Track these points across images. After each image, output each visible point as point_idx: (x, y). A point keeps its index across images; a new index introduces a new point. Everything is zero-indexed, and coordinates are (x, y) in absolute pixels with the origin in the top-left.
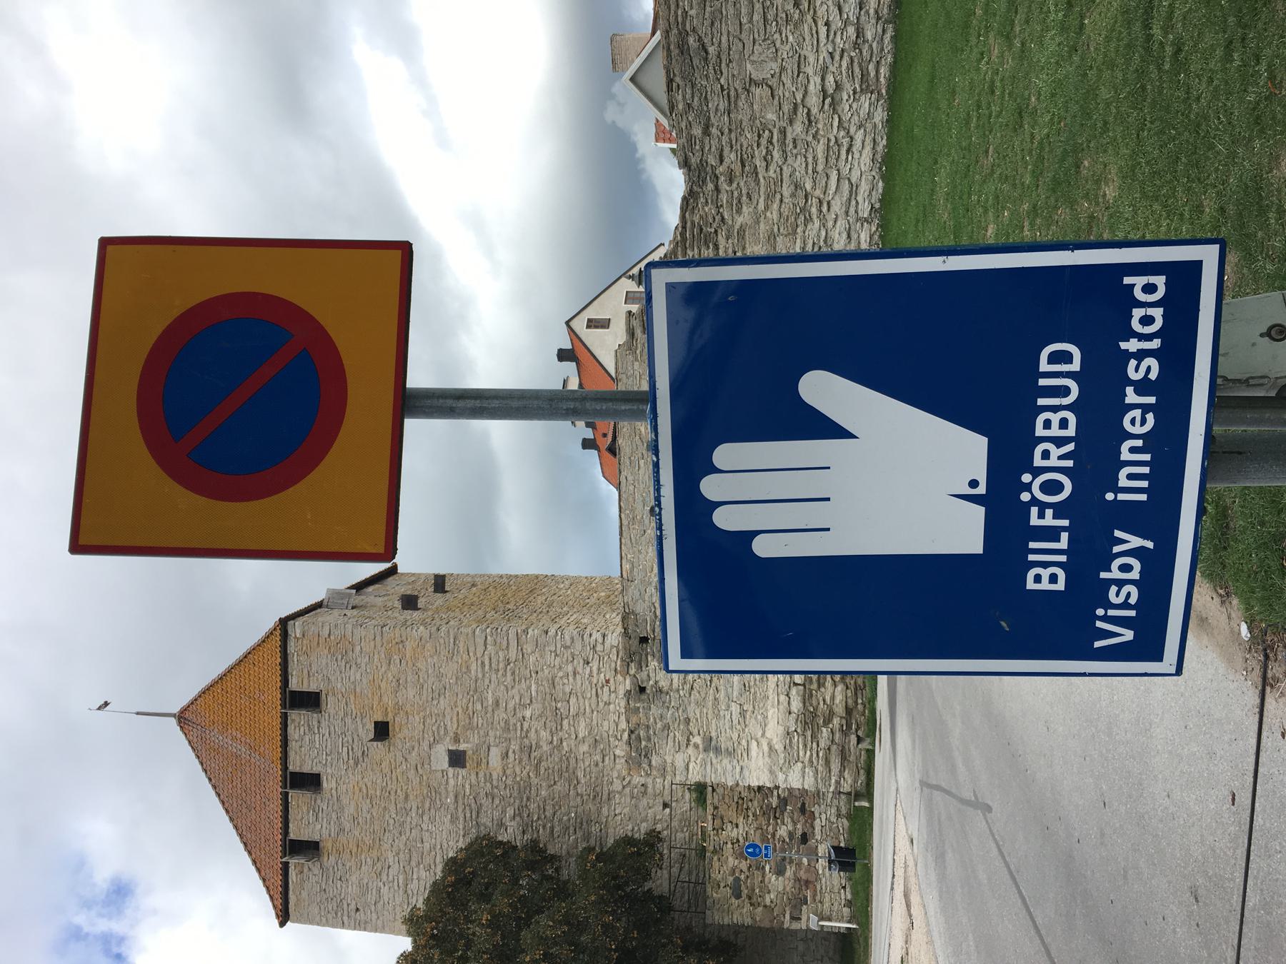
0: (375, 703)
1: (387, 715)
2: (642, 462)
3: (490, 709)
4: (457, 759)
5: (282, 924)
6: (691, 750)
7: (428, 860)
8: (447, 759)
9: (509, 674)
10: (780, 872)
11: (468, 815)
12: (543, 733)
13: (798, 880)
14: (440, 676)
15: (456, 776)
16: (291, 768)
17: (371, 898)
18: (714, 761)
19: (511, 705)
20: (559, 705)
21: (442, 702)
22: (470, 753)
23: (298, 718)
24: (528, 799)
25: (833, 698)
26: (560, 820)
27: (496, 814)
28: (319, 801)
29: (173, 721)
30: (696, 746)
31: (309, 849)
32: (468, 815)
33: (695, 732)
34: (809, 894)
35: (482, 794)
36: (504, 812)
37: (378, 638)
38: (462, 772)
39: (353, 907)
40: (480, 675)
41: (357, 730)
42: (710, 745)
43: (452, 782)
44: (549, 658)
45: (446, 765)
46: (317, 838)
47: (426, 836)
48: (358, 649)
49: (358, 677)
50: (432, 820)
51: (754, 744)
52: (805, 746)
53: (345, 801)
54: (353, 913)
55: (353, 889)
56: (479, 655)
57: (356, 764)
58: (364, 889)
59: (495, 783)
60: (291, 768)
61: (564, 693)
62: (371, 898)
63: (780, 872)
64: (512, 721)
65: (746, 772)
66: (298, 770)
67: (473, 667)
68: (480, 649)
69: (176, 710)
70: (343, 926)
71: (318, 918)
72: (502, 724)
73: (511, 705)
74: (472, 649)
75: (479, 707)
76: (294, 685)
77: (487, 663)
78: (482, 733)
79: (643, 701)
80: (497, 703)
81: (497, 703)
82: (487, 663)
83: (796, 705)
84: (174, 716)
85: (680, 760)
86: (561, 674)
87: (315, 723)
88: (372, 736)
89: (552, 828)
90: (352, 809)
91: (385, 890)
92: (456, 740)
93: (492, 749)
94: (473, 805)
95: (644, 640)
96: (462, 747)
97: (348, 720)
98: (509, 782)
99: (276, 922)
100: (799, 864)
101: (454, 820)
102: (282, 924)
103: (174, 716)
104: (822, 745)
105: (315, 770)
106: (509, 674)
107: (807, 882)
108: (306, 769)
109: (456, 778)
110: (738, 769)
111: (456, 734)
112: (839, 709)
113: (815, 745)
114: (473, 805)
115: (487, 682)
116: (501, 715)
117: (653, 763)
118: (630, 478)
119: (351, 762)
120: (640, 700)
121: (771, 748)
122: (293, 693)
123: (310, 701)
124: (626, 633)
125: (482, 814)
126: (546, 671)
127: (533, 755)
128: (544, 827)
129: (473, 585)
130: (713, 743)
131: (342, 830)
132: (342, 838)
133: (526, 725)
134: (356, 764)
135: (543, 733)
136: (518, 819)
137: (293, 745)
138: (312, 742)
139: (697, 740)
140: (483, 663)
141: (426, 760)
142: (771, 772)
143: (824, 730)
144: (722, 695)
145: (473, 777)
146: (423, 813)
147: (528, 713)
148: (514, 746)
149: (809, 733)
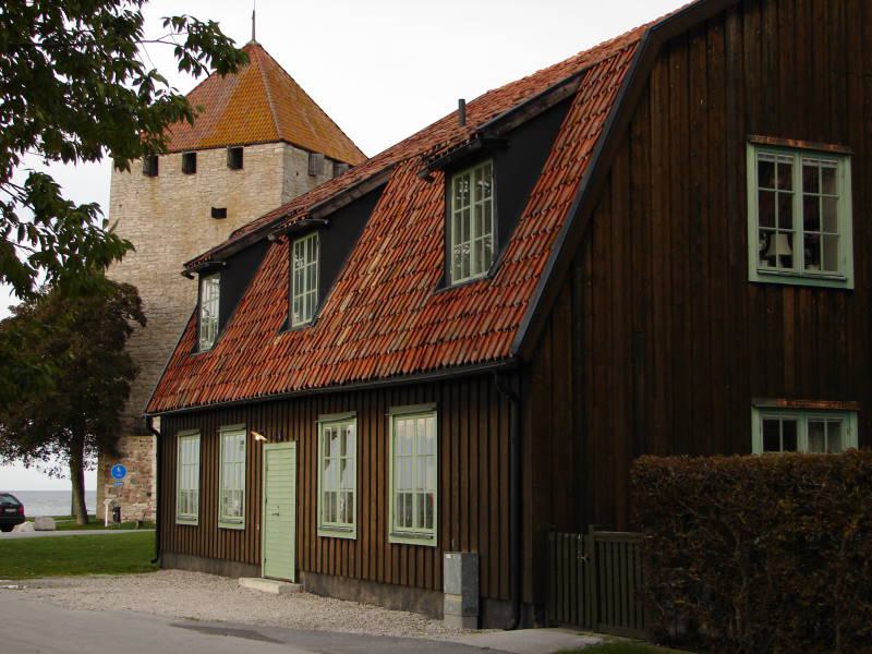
7: (150, 251)
10: (132, 481)
13: (130, 491)
16: (199, 153)
27: (176, 295)
29: (249, 39)
34: (122, 498)
36: (178, 300)
39: (122, 203)
46: (160, 175)
47: (162, 249)
48: (268, 193)
53: (181, 192)
57: (201, 198)
60: (199, 153)
63: (132, 481)
66: (198, 158)
69: (258, 40)
70: (111, 197)
84: (254, 39)
89: (169, 333)
90: (176, 197)
91: (131, 224)
100: (136, 492)
103: (254, 39)
105: (198, 170)
107: (127, 497)
122: (241, 150)
123: (236, 161)
131: (164, 191)
132: (160, 192)
134: (201, 198)
138: (213, 166)
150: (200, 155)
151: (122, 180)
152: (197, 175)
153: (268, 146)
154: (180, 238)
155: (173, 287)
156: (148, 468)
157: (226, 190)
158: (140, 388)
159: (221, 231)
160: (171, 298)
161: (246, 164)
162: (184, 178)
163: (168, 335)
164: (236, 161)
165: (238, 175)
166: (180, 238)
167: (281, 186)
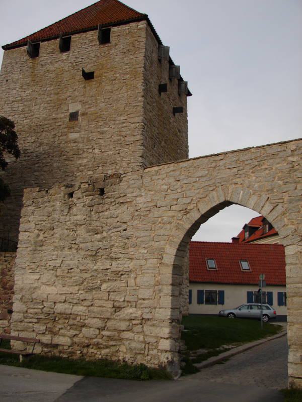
0: (103, 71)
1: (96, 77)
2: (235, 170)
3: (99, 130)
4: (74, 116)
5: (3, 47)
6: (37, 231)
8: (74, 111)
9: (118, 138)
11: (45, 126)
12: (85, 161)
14: (118, 100)
15: (65, 117)
17: (12, 86)
18: (29, 249)
19: (101, 141)
20: (100, 168)
21: (103, 104)
22: (76, 122)
23: (94, 35)
24: (52, 156)
25: (64, 336)
26: (42, 175)
28: (57, 53)
30: (38, 235)
31: (34, 52)
32: (45, 126)
33: (46, 235)
35: (56, 132)
36: (47, 145)
37: (137, 66)
38: (67, 120)
39: (9, 78)
40: (117, 122)
41: (91, 63)
42: (38, 245)
43: (63, 115)
44: (127, 160)
45: (71, 111)
46: (40, 55)
47: (37, 107)
48: (131, 57)
49: (117, 60)
50: (45, 108)
51: (37, 277)
52: (36, 314)
53: (56, 65)
54: (6, 79)
55: (16, 76)
56: (128, 120)
58: (15, 82)
59: (61, 138)
61: (107, 170)
62: (12, 86)
64: (93, 143)
65: (22, 271)
66: (72, 40)
67: (122, 118)
68: (132, 120)
71: (4, 63)
72: (91, 138)
73: (101, 141)
74: (131, 116)
75: (100, 124)
76: (114, 29)
77: (124, 125)
78: (86, 127)
79: (64, 197)
80: (102, 133)
81: (102, 133)
82: (124, 125)
83: (60, 308)
85: (32, 225)
86: (118, 167)
87: (94, 44)
88: (87, 71)
89: (38, 171)
91: (14, 92)
92: (83, 114)
93: (78, 134)
94: (50, 128)
95: (102, 192)
96: (80, 118)
97: (95, 59)
98: (61, 145)
99: (5, 44)
101: (45, 119)
102: (3, 47)
104: (36, 326)
105: (72, 49)
106: (118, 138)
108: (72, 44)
109: (64, 116)
110: (24, 266)
111: (87, 113)
112: (58, 340)
113: (36, 320)
114: (50, 128)
115: (113, 127)
116: (95, 136)
117: (30, 208)
118: (221, 163)
119: (74, 64)
120: (65, 194)
121: (35, 288)
122: (109, 30)
123: (105, 38)
124: (107, 177)
125: (46, 133)
126: (119, 159)
127: (75, 156)
128: (38, 167)
129: (179, 131)
130: (38, 248)
132: (39, 67)
133: (91, 150)
135: (85, 161)
136: (44, 152)
137: (83, 35)
139: (41, 238)
140: (124, 123)
141: (74, 100)
142: (22, 289)
143: (45, 327)
144: (67, 252)
145: (64, 126)
146: (49, 103)
147: (96, 151)
148: (80, 146)
149: (42, 316)
150: (74, 38)
151: (11, 63)
152: (71, 51)
153: (133, 25)
154: (54, 97)
155: (44, 134)
156: (10, 283)
157: (95, 59)
158: (9, 217)
159: (88, 88)
160: (41, 144)
161: (113, 39)
162: (59, 55)
163: (37, 173)
164: (105, 38)
165: (105, 48)
166: (54, 97)
167: (144, 50)
